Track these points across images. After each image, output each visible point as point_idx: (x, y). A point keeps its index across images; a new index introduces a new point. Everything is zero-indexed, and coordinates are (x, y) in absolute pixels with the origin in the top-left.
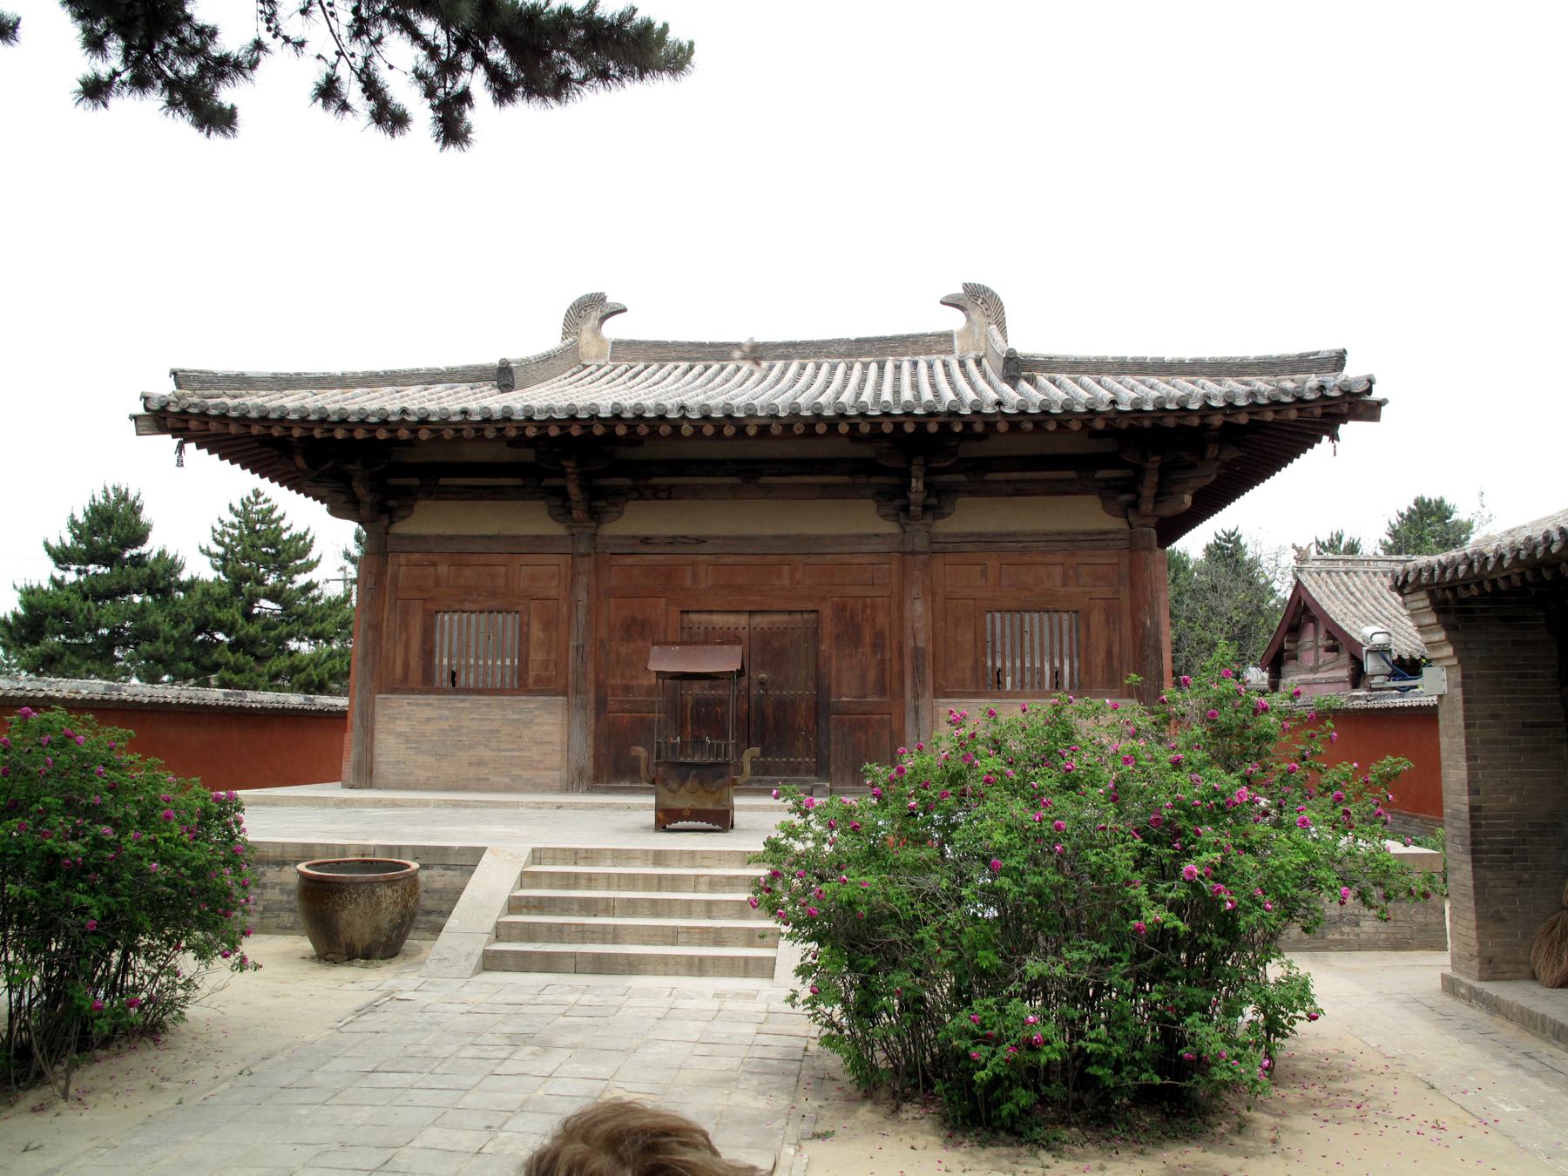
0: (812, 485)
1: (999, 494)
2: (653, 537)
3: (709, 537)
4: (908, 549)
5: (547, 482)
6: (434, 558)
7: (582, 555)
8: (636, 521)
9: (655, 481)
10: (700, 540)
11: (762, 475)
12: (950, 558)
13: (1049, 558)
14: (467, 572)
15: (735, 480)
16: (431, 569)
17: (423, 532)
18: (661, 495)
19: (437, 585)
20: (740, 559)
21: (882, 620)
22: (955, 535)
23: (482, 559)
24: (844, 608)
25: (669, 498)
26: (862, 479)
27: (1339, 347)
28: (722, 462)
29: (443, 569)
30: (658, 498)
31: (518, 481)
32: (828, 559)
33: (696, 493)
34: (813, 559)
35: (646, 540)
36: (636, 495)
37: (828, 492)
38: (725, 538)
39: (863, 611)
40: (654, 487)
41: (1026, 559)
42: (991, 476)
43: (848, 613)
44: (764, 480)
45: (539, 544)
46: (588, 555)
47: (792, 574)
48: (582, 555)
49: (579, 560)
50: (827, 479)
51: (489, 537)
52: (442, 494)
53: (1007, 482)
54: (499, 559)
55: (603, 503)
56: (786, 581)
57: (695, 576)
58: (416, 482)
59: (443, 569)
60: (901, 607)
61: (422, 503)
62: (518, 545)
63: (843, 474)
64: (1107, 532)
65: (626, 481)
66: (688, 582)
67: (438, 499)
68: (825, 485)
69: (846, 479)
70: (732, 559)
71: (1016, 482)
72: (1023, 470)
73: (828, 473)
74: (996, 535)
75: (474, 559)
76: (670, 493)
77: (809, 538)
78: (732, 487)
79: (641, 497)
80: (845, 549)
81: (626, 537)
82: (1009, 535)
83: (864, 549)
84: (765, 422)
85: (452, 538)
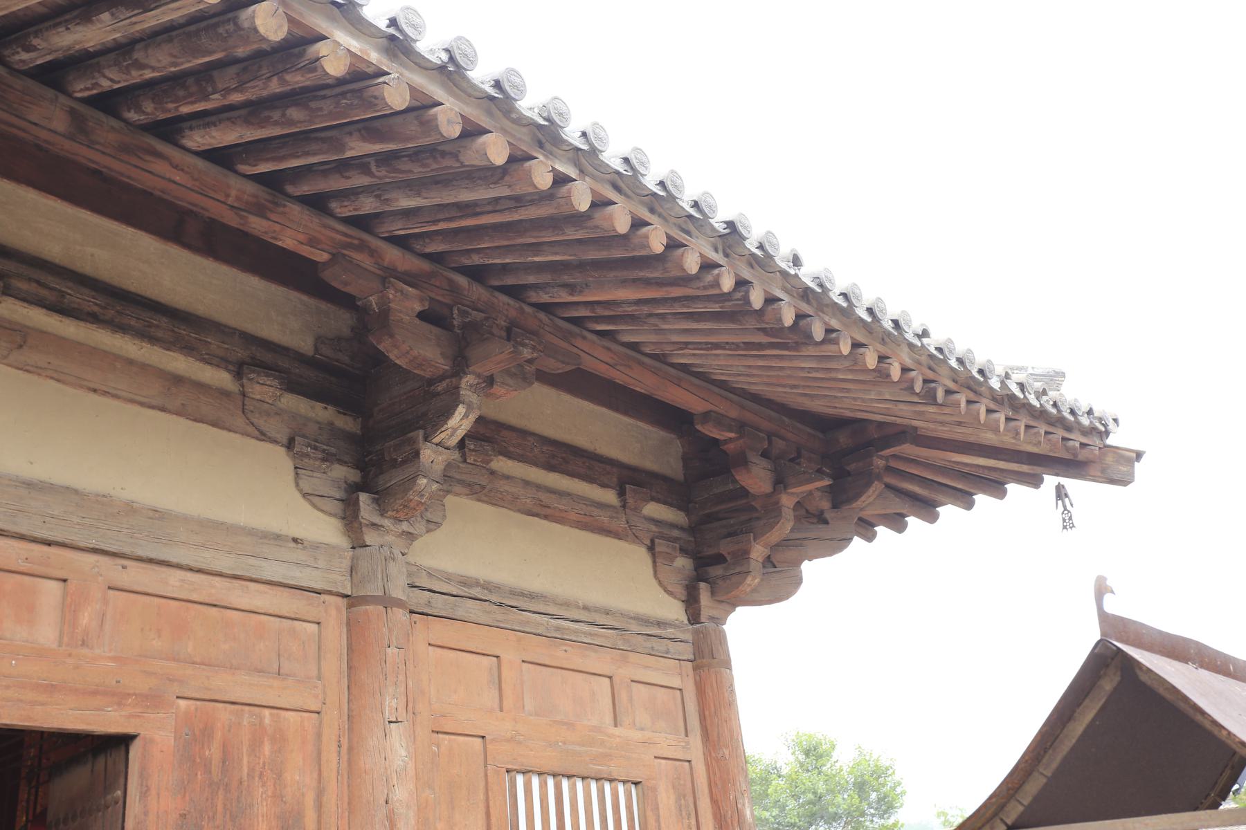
0: (145, 368)
1: (511, 503)
4: (374, 590)
12: (441, 631)
13: (594, 661)
21: (298, 775)
22: (448, 578)
24: (207, 732)
26: (263, 389)
27: (1059, 367)
32: (174, 581)
34: (137, 575)
37: (179, 398)
39: (256, 744)
41: (560, 654)
42: (502, 464)
43: (214, 752)
47: (69, 610)
50: (179, 363)
53: (527, 483)
56: (46, 633)
60: (352, 749)
63: (221, 362)
64: (660, 624)
68: (177, 380)
69: (221, 378)
71: (539, 487)
72: (550, 468)
73: (188, 349)
74: (515, 593)
77: (130, 509)
80: (224, 563)
82: (532, 596)
83: (271, 571)
84: (374, 57)
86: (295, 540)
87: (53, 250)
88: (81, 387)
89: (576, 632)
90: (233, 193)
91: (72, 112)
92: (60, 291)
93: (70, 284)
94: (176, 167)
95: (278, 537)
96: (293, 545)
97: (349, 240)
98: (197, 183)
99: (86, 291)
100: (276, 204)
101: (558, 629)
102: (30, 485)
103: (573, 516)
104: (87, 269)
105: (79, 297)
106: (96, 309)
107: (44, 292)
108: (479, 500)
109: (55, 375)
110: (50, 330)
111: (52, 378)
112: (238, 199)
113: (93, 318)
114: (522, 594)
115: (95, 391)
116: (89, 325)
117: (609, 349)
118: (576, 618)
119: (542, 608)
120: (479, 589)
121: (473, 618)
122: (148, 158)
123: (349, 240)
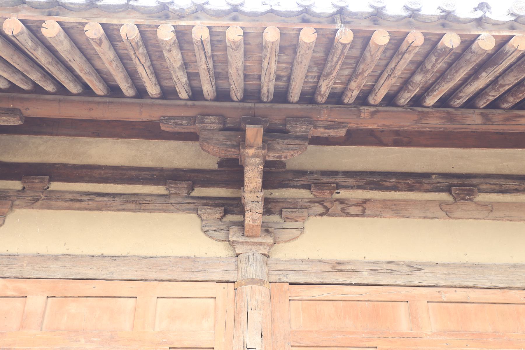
2: (349, 262)
3: (424, 264)
5: (198, 192)
6: (23, 285)
7: (253, 281)
8: (321, 240)
9: (344, 194)
10: (415, 268)
11: (480, 191)
14: (73, 307)
15: (444, 196)
16: (18, 303)
17: (13, 251)
18: (352, 210)
19: (22, 327)
20: (473, 295)
23: (99, 288)
25: (363, 215)
28: (427, 175)
29: (36, 302)
30: (348, 214)
31: (161, 190)
33: (397, 210)
35: (338, 266)
36: (321, 210)
38: (447, 265)
40: (341, 201)
44: (481, 197)
45: (183, 271)
46: (261, 282)
48: (253, 281)
49: (247, 289)
51: (114, 258)
52: (51, 200)
54: (125, 288)
55: (275, 218)
57: (413, 317)
58: (16, 185)
59: (36, 302)
61: (17, 211)
62: (156, 273)
65: (305, 194)
66: (404, 326)
67: (43, 207)
70: (461, 294)
75: (89, 288)
76: (364, 209)
78: (441, 205)
79: (327, 212)
81: (310, 262)
85: (57, 258)
87: (492, 169)
88: (521, 220)
91: (482, 114)
92: (499, 184)
93: (503, 180)
99: (509, 181)
102: (514, 266)
104: (507, 172)
105: (508, 184)
106: (516, 187)
107: (493, 187)
109: (509, 218)
110: (501, 201)
111: (508, 220)
113: (517, 191)
116: (515, 194)
122: (518, 119)
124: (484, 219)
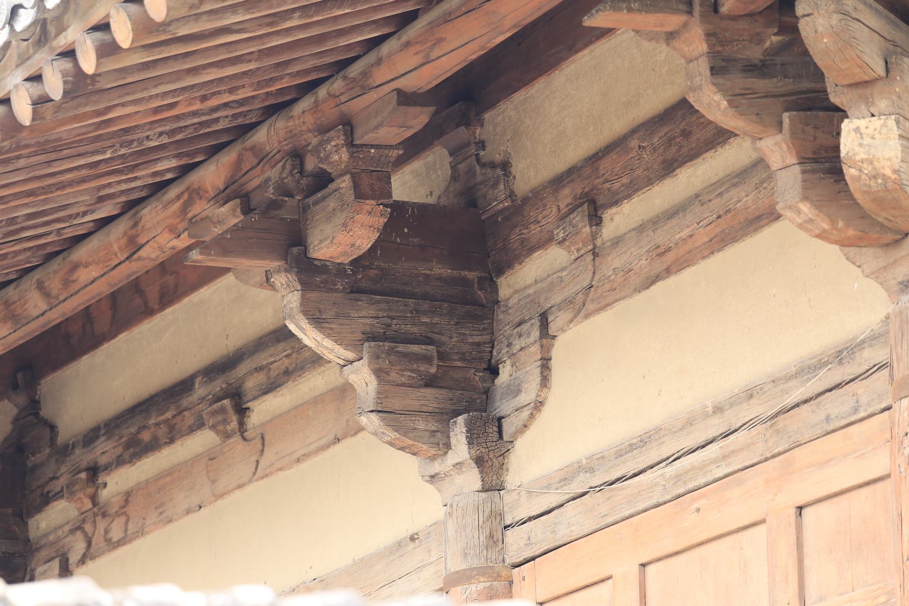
71: (655, 222)
72: (669, 168)
86: (412, 539)
89: (702, 467)
90: (115, 247)
94: (86, 266)
95: (399, 544)
96: (412, 545)
97: (182, 201)
98: (101, 265)
100: (136, 224)
101: (678, 477)
103: (703, 237)
108: (587, 317)
112: (121, 249)
114: (632, 447)
115: (298, 460)
117: (408, 44)
118: (701, 440)
119: (666, 451)
120: (582, 477)
121: (577, 531)
123: (182, 201)
124: (250, 481)
